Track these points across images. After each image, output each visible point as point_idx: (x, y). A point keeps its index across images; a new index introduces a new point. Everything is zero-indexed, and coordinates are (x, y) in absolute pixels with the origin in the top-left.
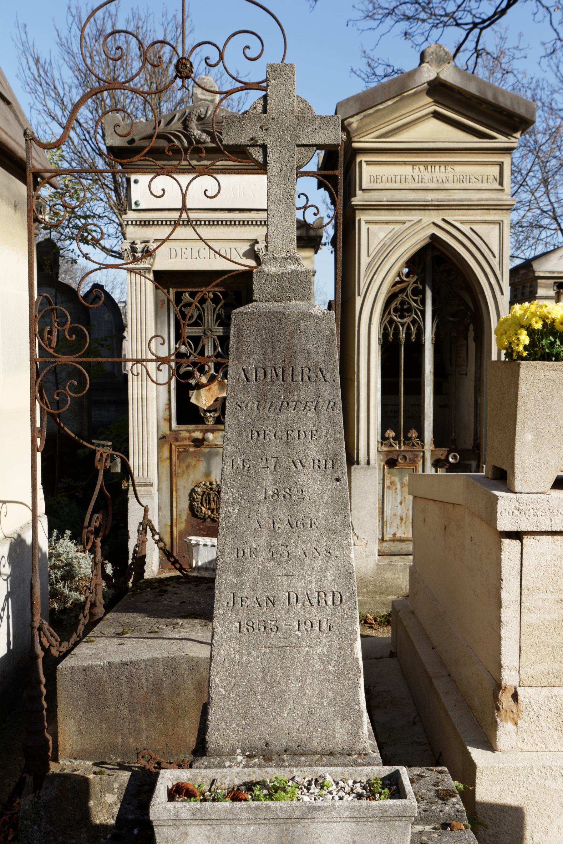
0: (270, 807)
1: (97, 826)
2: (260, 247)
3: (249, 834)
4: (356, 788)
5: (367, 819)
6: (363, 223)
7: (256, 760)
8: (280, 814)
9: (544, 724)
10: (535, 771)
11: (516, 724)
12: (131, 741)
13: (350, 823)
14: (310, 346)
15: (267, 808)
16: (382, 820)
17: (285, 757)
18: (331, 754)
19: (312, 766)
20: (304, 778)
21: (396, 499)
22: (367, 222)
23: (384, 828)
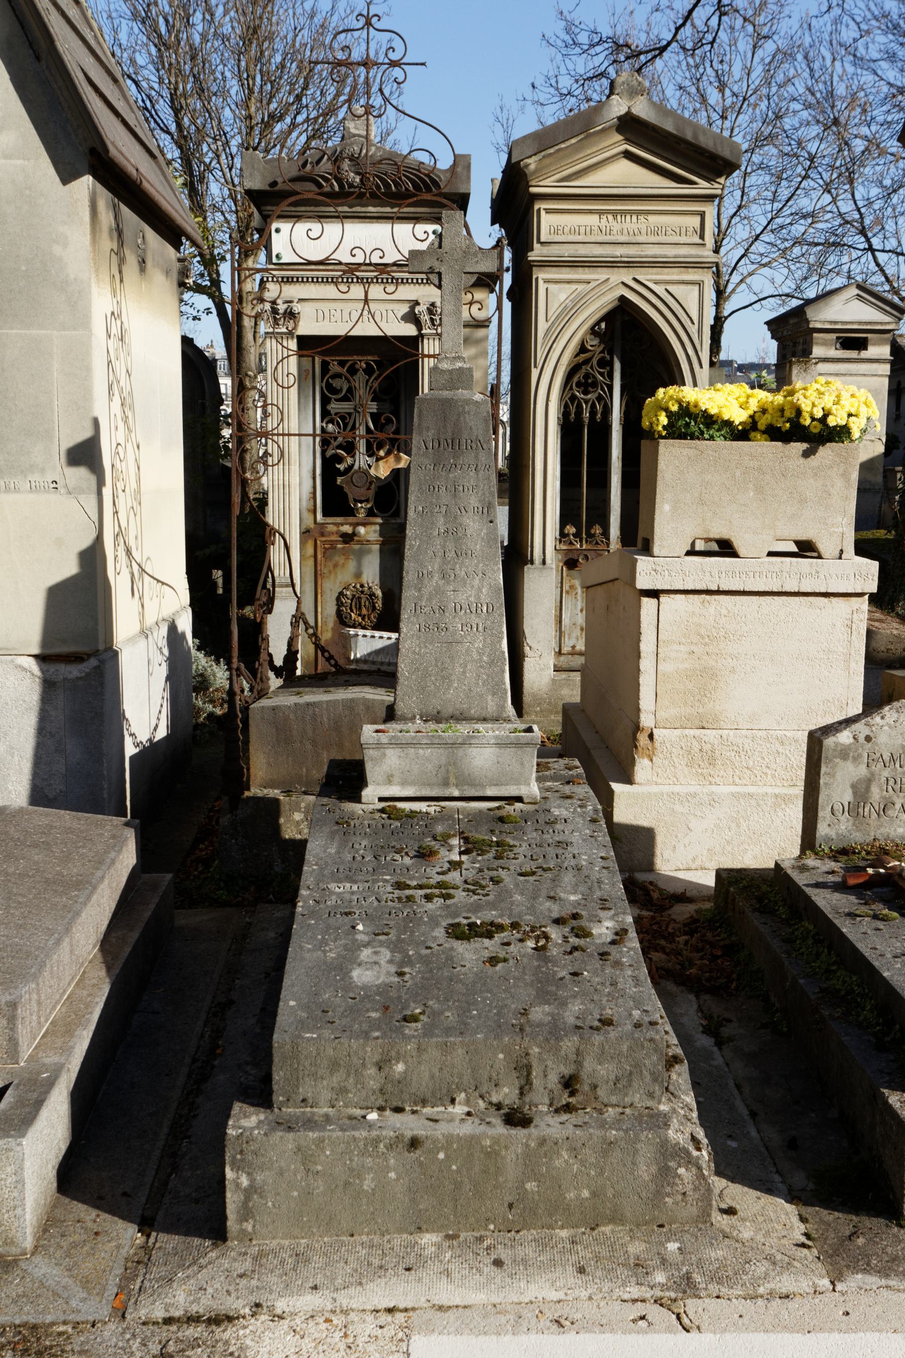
1: (286, 840)
2: (421, 309)
3: (427, 755)
6: (541, 282)
9: (676, 760)
10: (665, 796)
11: (651, 760)
12: (314, 772)
14: (472, 424)
21: (576, 606)
22: (546, 281)
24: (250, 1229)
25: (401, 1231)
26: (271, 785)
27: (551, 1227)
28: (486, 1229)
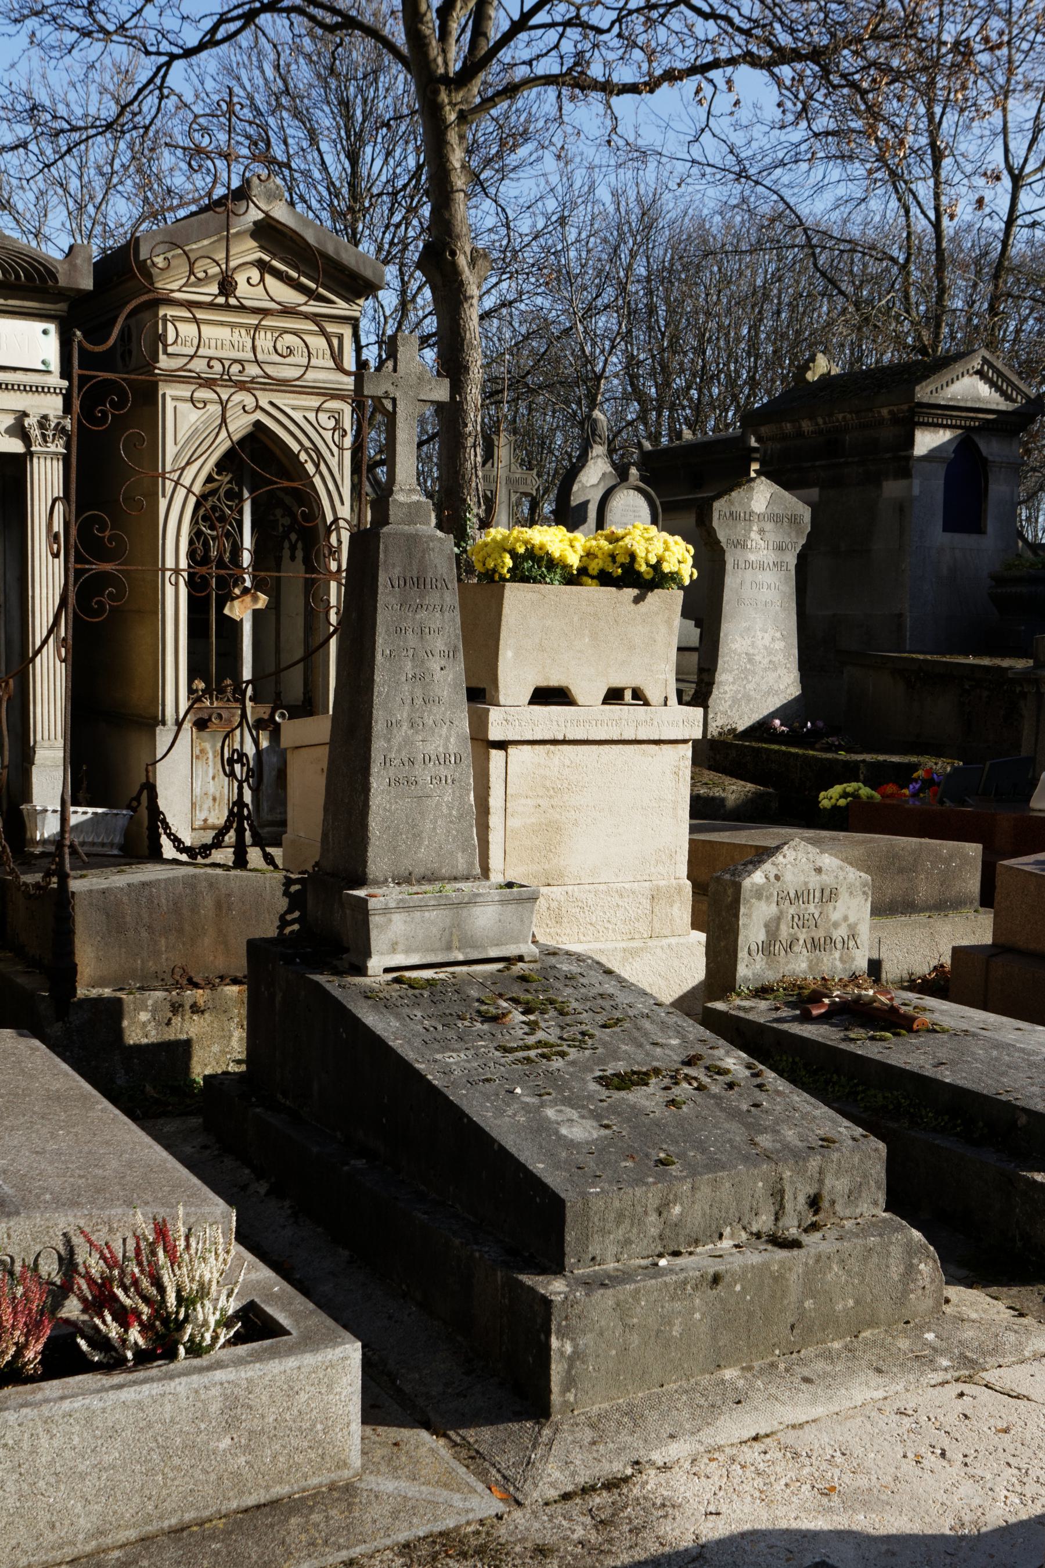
1: (130, 1046)
2: (31, 422)
6: (168, 399)
14: (437, 561)
21: (207, 772)
22: (175, 399)
24: (572, 1399)
25: (703, 1371)
26: (101, 983)
27: (824, 1342)
28: (773, 1354)
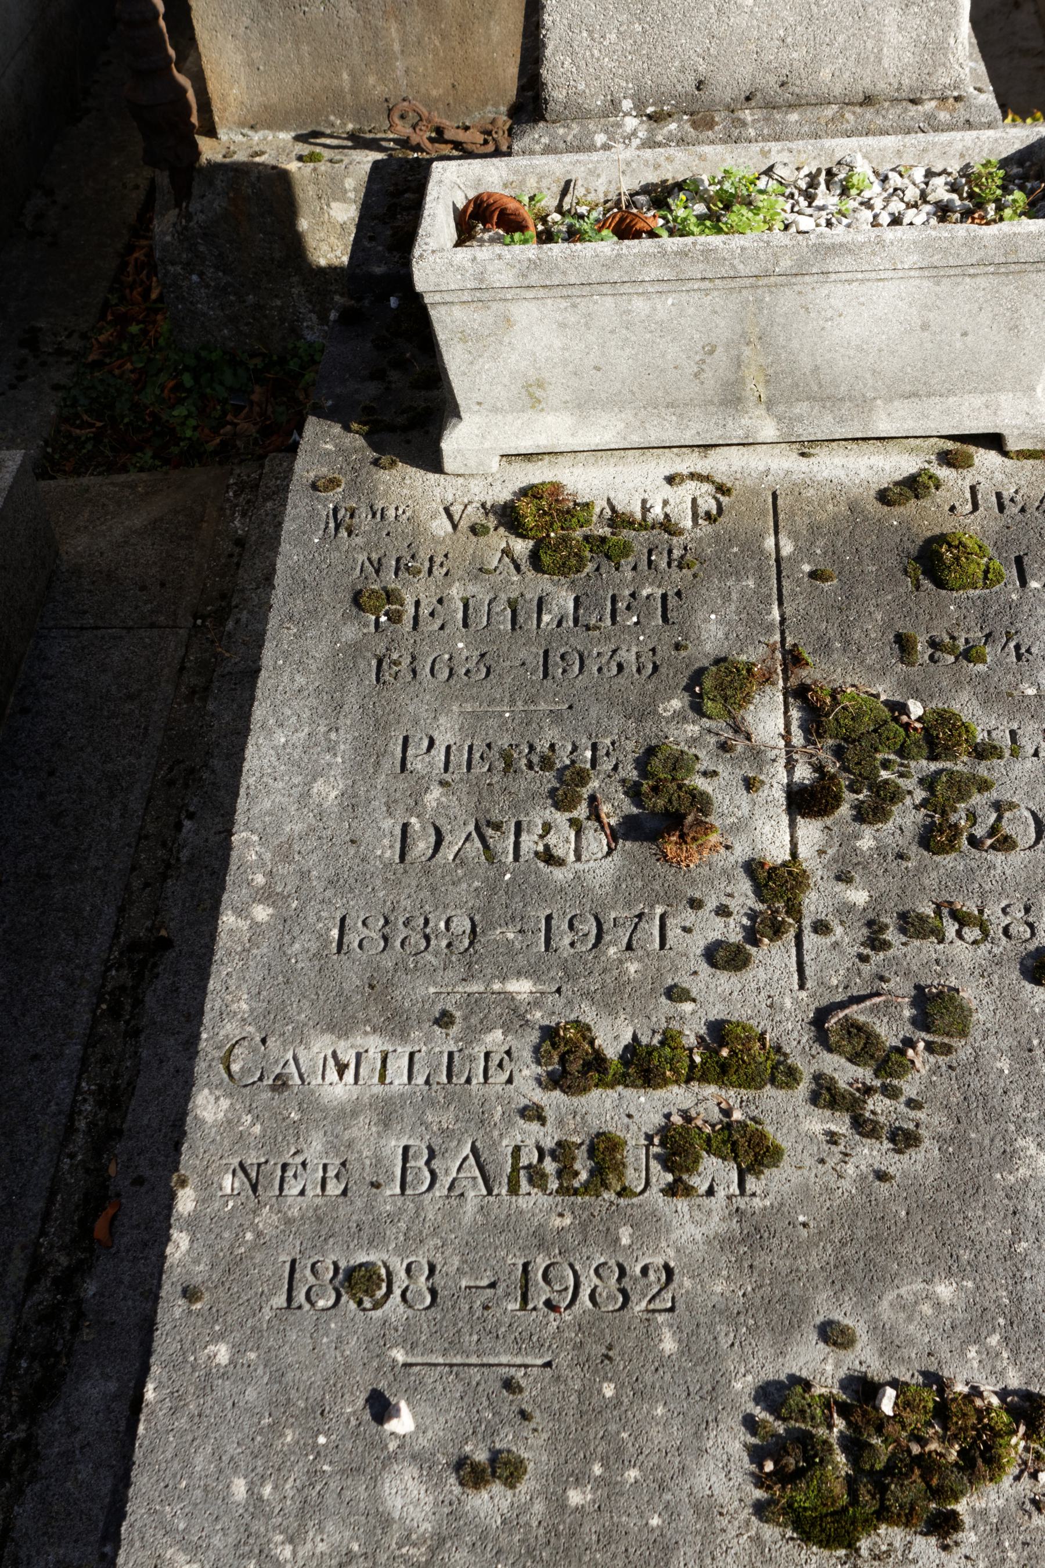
0: (715, 250)
1: (321, 270)
3: (661, 314)
4: (934, 191)
5: (964, 271)
7: (673, 126)
8: (741, 267)
12: (371, 80)
13: (918, 281)
15: (707, 252)
16: (1003, 270)
17: (747, 115)
18: (868, 100)
19: (817, 136)
20: (798, 169)
23: (1005, 290)
